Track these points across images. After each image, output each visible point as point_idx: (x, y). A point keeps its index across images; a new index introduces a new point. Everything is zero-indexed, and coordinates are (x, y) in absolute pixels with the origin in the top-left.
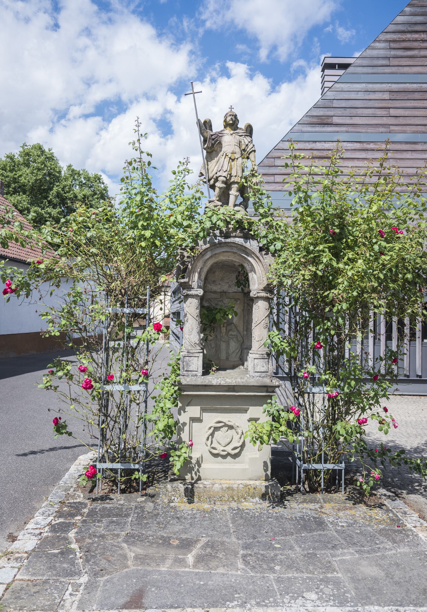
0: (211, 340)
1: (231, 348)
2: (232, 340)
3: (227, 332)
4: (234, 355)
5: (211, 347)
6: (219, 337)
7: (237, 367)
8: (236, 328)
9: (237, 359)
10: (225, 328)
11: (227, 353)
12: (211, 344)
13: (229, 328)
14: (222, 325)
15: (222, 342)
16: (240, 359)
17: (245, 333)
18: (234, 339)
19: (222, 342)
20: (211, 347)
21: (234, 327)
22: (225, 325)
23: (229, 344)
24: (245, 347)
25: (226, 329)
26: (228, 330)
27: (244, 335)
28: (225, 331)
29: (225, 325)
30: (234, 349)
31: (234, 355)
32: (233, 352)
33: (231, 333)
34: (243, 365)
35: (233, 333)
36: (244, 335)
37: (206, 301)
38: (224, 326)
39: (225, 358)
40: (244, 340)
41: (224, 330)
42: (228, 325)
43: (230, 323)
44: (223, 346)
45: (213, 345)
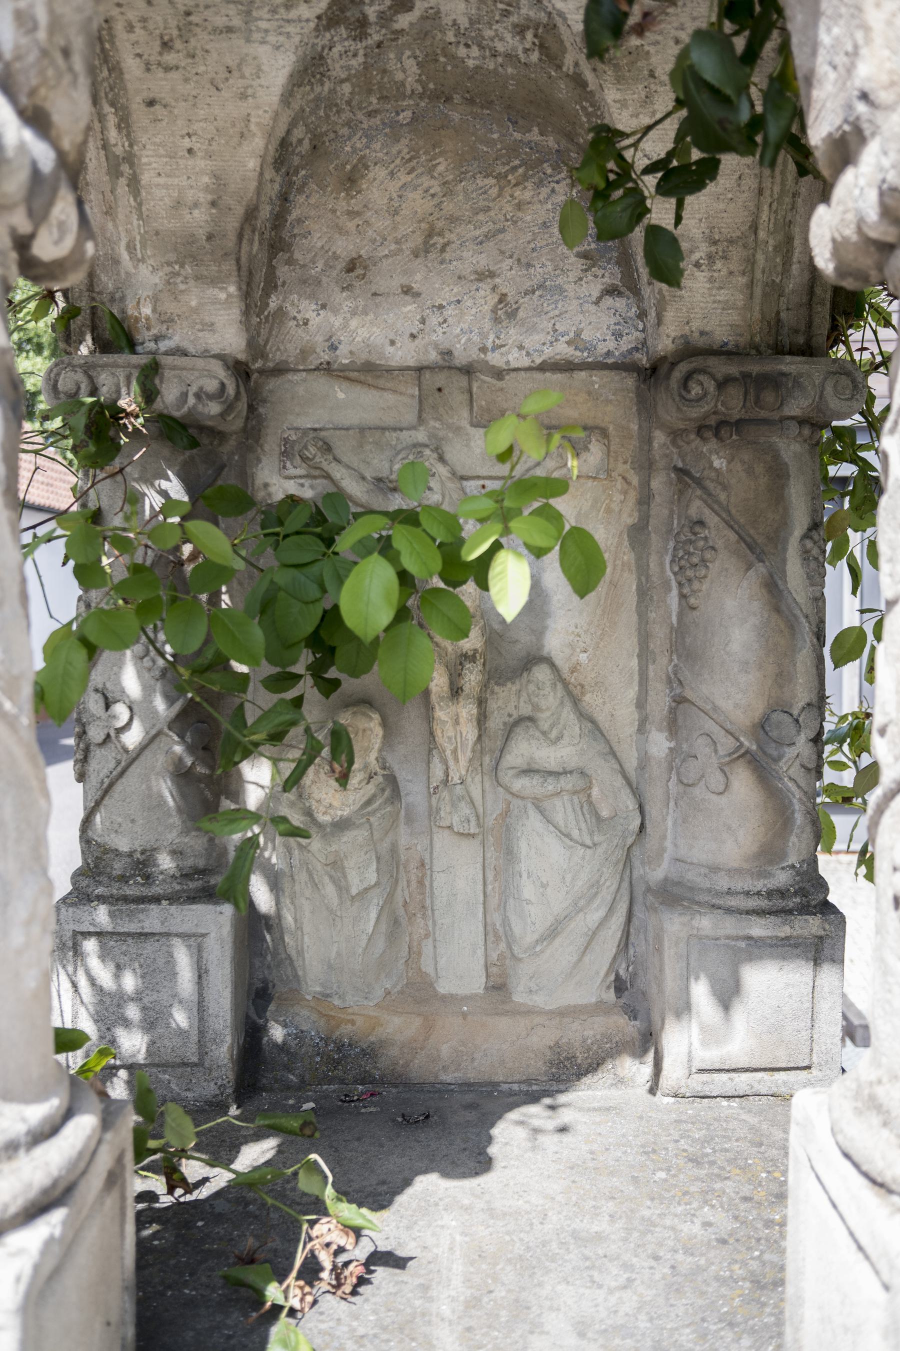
0: (342, 825)
1: (528, 890)
2: (534, 821)
3: (493, 742)
4: (563, 952)
5: (342, 888)
6: (414, 791)
7: (593, 1066)
8: (574, 697)
9: (591, 988)
10: (467, 710)
11: (496, 933)
12: (336, 865)
13: (506, 702)
14: (439, 682)
15: (442, 840)
16: (620, 986)
17: (659, 744)
18: (563, 811)
19: (442, 840)
20: (342, 888)
21: (550, 699)
22: (472, 678)
23: (509, 853)
24: (657, 874)
25: (482, 719)
26: (495, 723)
27: (644, 763)
28: (470, 732)
29: (472, 678)
30: (558, 902)
31: (563, 952)
32: (552, 933)
33: (524, 749)
34: (647, 1042)
35: (549, 756)
36: (644, 763)
37: (287, 452)
38: (456, 691)
39: (476, 984)
40: (654, 811)
41: (456, 724)
42: (496, 676)
43: (511, 658)
44: (457, 872)
45: (362, 873)
